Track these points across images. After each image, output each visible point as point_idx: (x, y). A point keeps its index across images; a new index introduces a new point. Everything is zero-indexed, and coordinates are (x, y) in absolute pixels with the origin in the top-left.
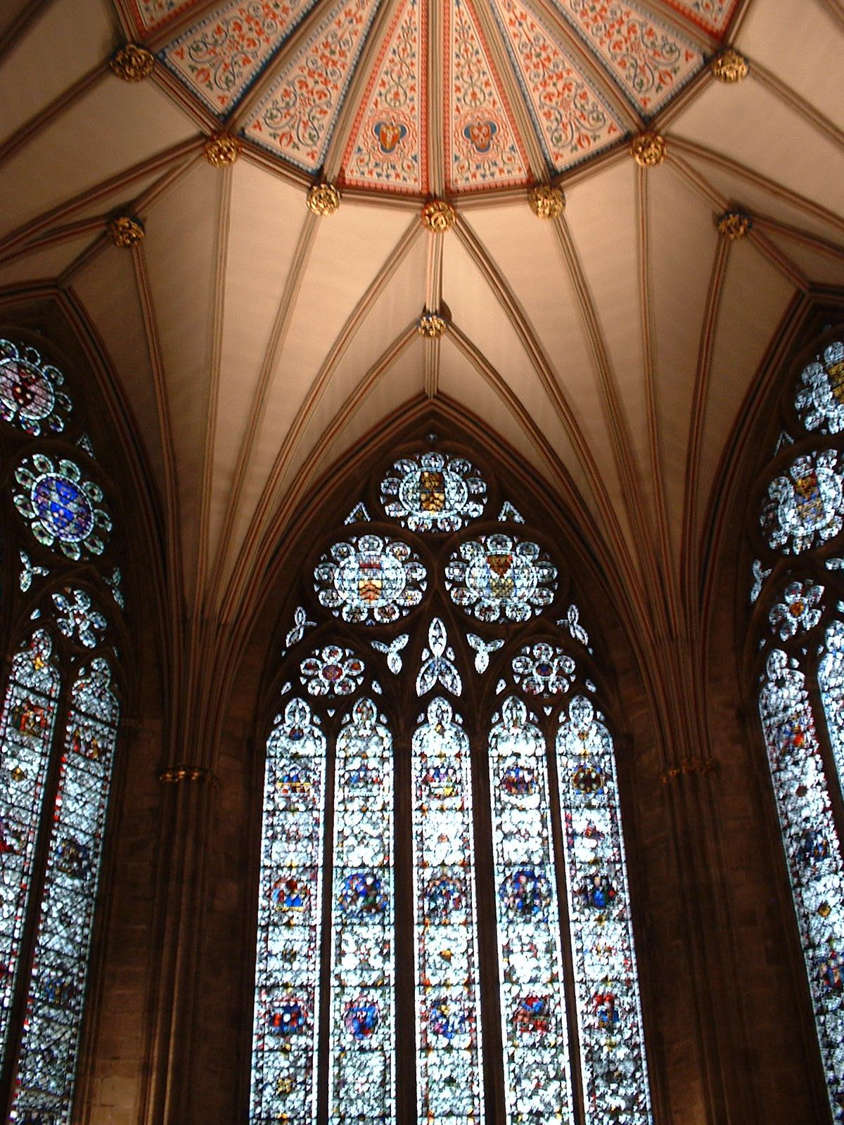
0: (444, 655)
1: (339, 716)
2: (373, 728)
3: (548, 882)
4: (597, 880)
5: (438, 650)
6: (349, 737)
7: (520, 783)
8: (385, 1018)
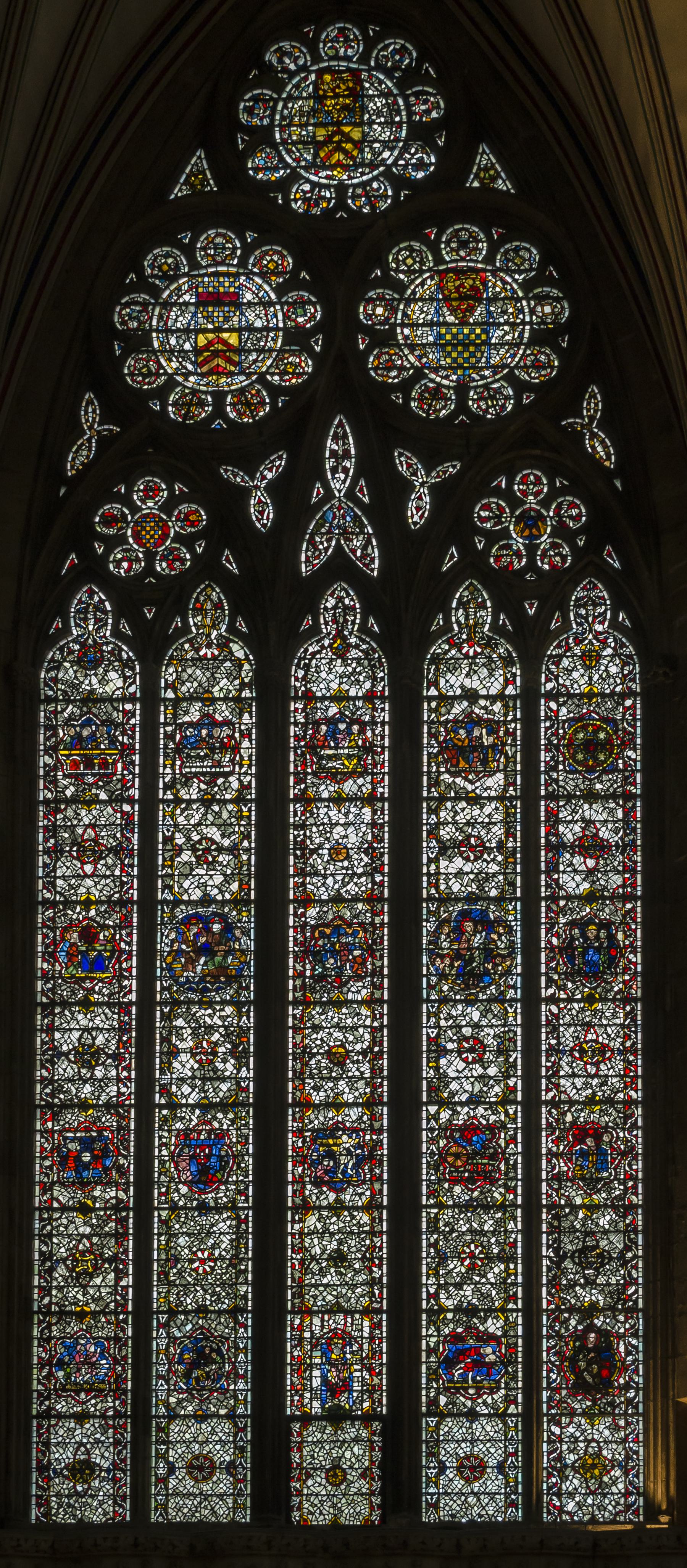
0: (350, 494)
1: (163, 618)
2: (224, 645)
3: (510, 931)
4: (592, 932)
5: (339, 484)
6: (182, 661)
7: (474, 749)
8: (238, 1157)
